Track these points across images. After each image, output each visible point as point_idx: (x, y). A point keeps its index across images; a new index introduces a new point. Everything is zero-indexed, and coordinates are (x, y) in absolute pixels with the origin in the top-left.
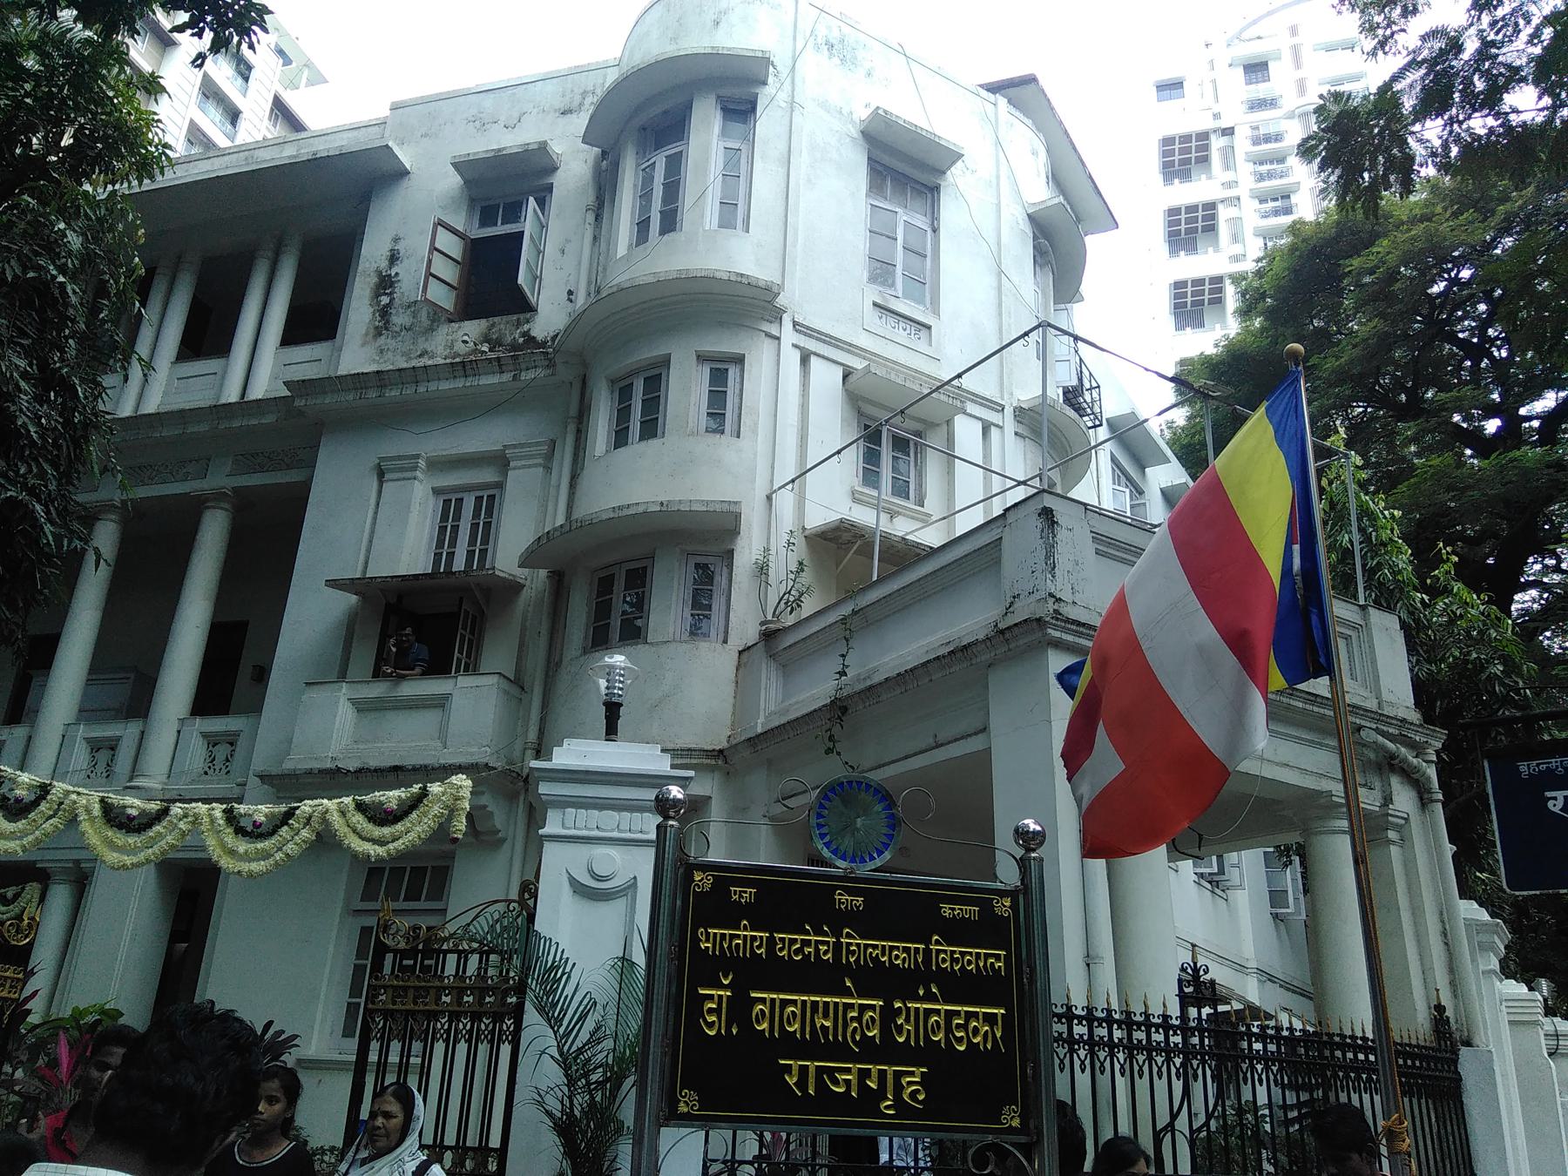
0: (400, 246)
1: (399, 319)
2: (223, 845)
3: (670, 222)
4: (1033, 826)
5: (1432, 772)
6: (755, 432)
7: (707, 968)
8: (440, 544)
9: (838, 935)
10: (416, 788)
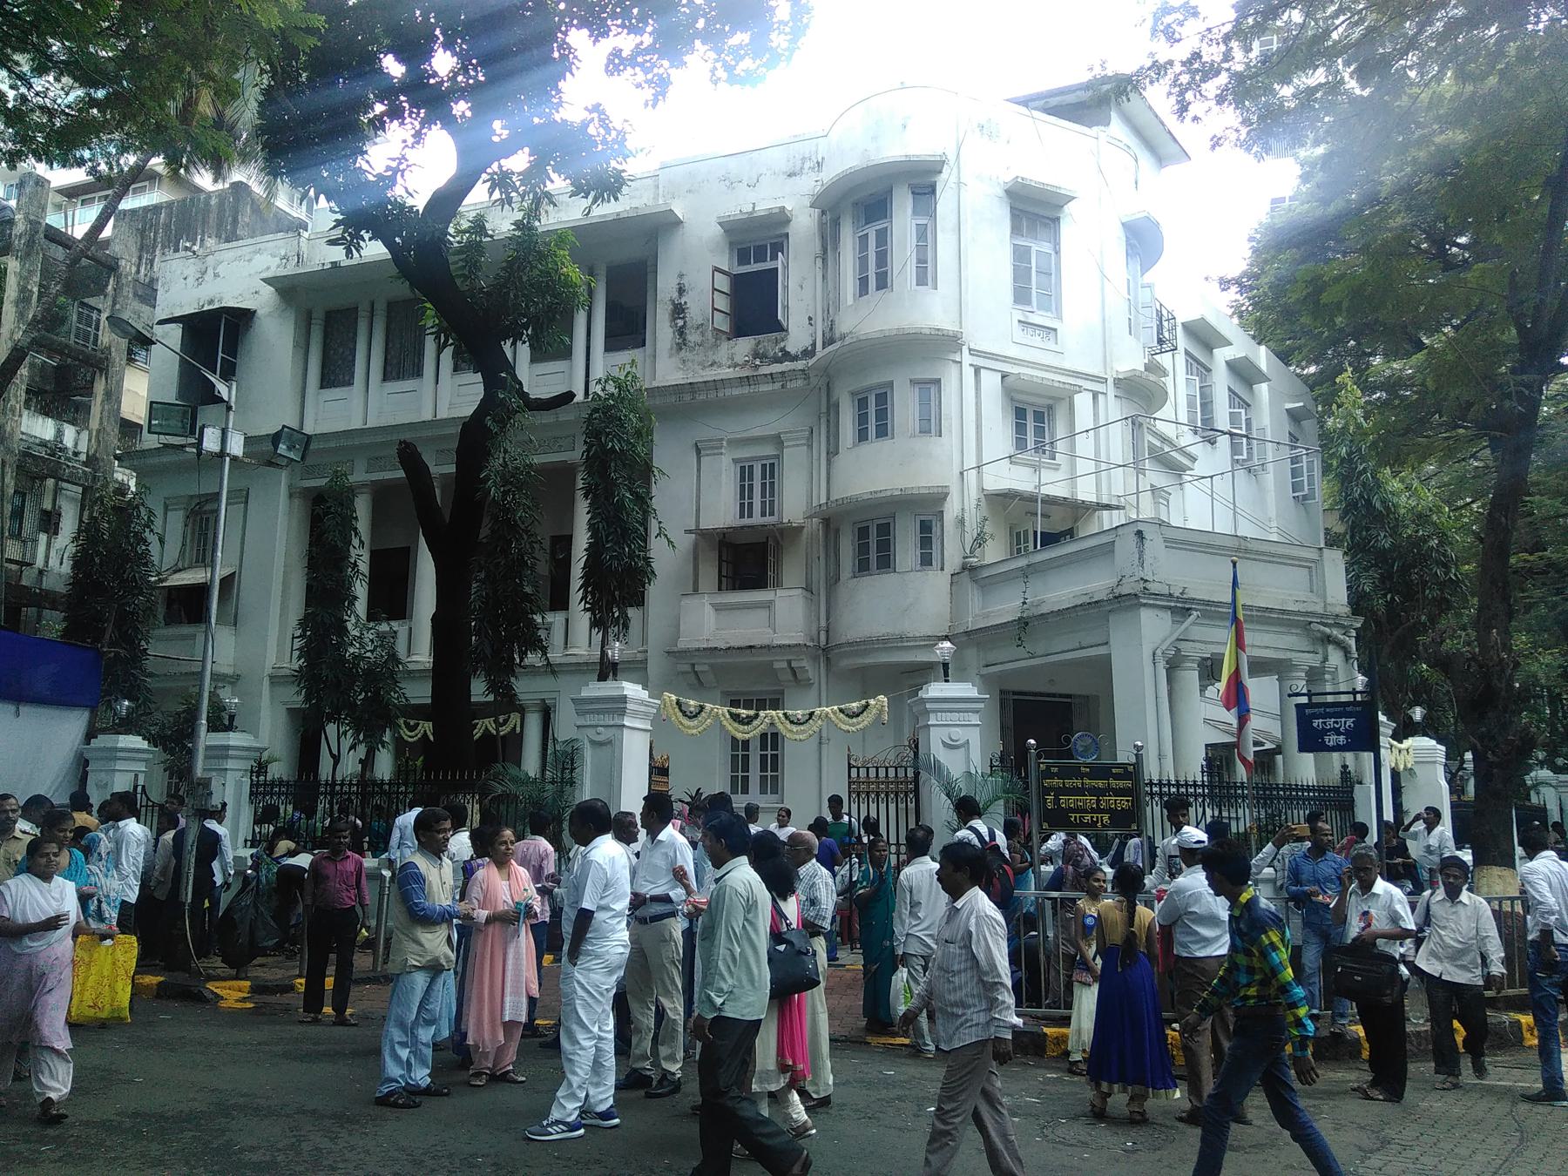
1: (693, 337)
2: (786, 728)
3: (883, 282)
4: (1139, 743)
5: (1352, 643)
7: (1047, 791)
8: (742, 497)
10: (863, 702)
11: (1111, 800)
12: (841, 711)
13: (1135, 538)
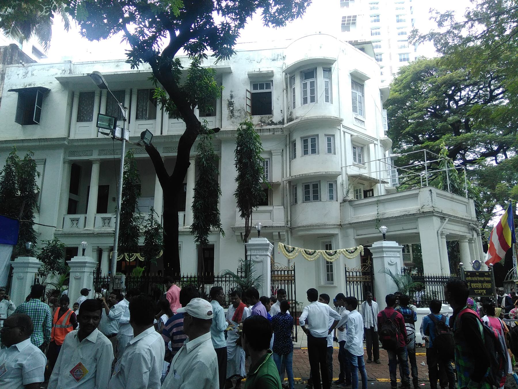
1: (236, 114)
3: (313, 100)
11: (485, 285)
12: (347, 250)
13: (430, 192)
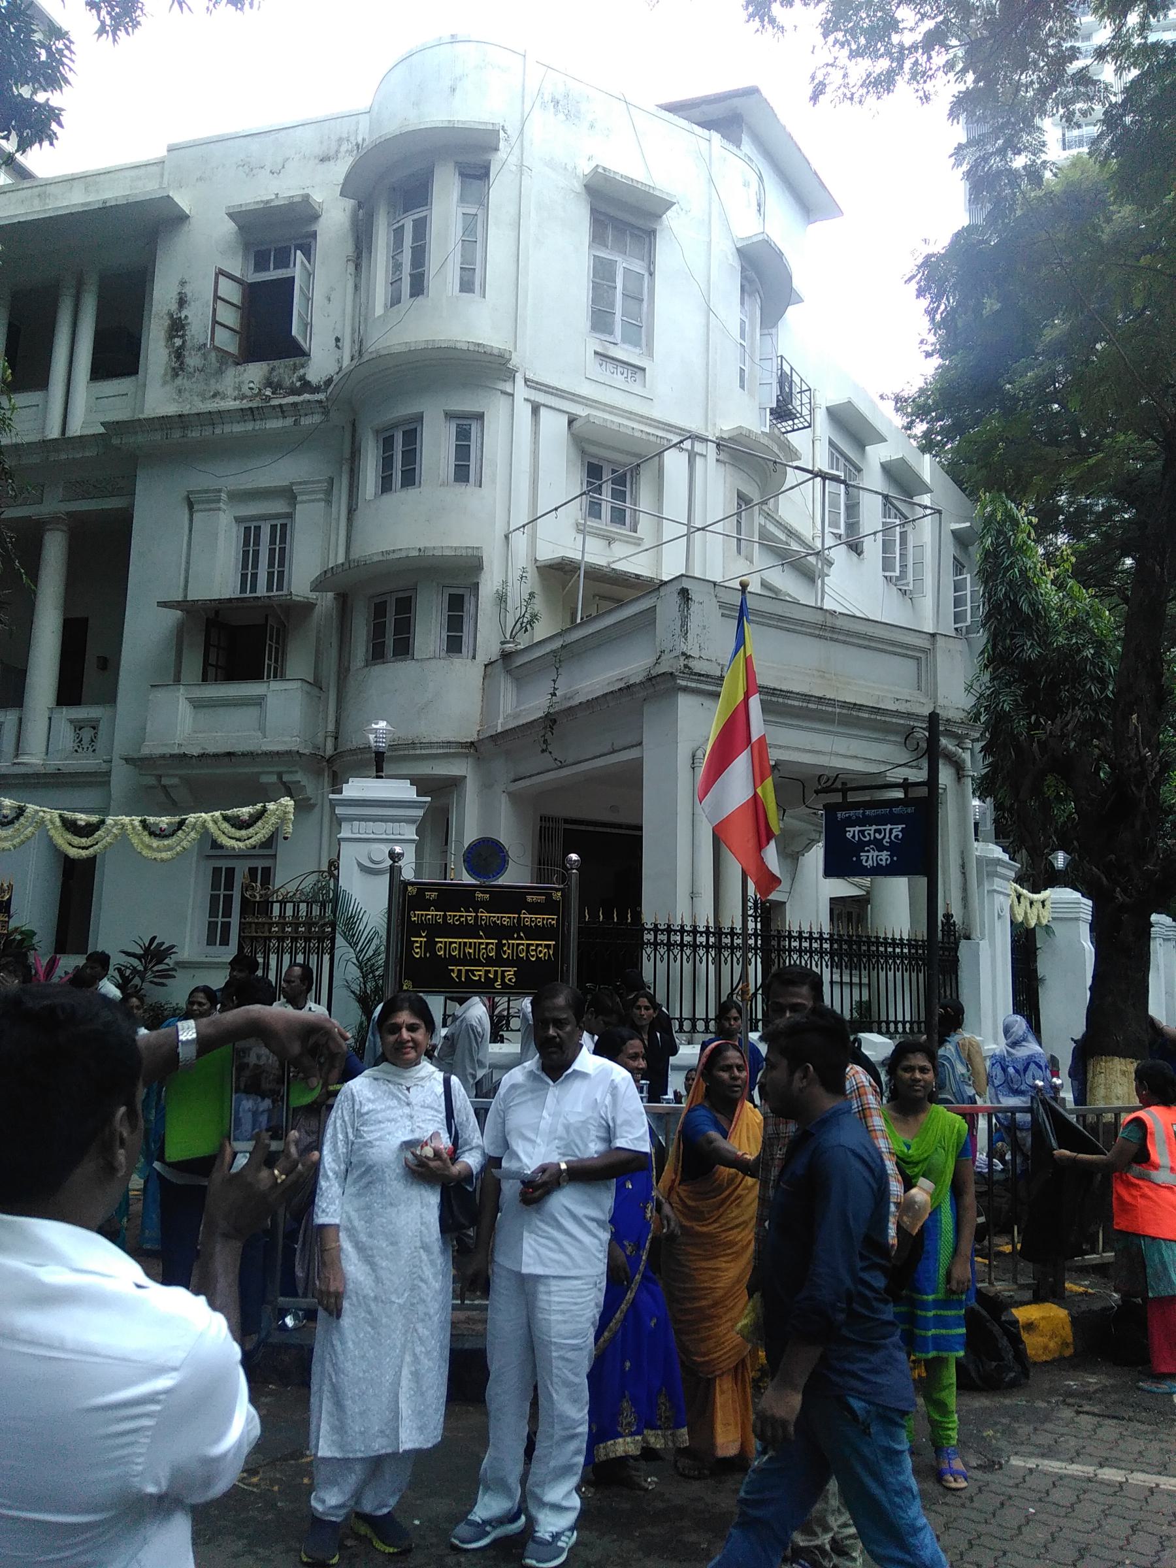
0: (187, 290)
1: (193, 360)
2: (142, 842)
3: (418, 287)
6: (494, 482)
7: (415, 929)
8: (245, 566)
9: (477, 912)
10: (259, 806)
11: (520, 945)
